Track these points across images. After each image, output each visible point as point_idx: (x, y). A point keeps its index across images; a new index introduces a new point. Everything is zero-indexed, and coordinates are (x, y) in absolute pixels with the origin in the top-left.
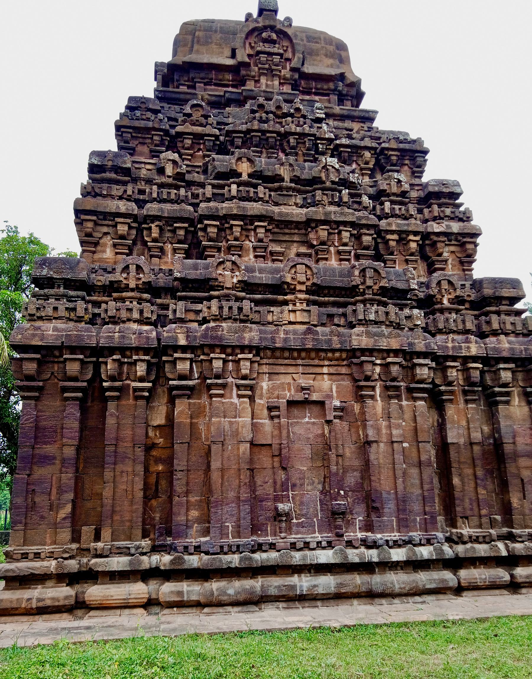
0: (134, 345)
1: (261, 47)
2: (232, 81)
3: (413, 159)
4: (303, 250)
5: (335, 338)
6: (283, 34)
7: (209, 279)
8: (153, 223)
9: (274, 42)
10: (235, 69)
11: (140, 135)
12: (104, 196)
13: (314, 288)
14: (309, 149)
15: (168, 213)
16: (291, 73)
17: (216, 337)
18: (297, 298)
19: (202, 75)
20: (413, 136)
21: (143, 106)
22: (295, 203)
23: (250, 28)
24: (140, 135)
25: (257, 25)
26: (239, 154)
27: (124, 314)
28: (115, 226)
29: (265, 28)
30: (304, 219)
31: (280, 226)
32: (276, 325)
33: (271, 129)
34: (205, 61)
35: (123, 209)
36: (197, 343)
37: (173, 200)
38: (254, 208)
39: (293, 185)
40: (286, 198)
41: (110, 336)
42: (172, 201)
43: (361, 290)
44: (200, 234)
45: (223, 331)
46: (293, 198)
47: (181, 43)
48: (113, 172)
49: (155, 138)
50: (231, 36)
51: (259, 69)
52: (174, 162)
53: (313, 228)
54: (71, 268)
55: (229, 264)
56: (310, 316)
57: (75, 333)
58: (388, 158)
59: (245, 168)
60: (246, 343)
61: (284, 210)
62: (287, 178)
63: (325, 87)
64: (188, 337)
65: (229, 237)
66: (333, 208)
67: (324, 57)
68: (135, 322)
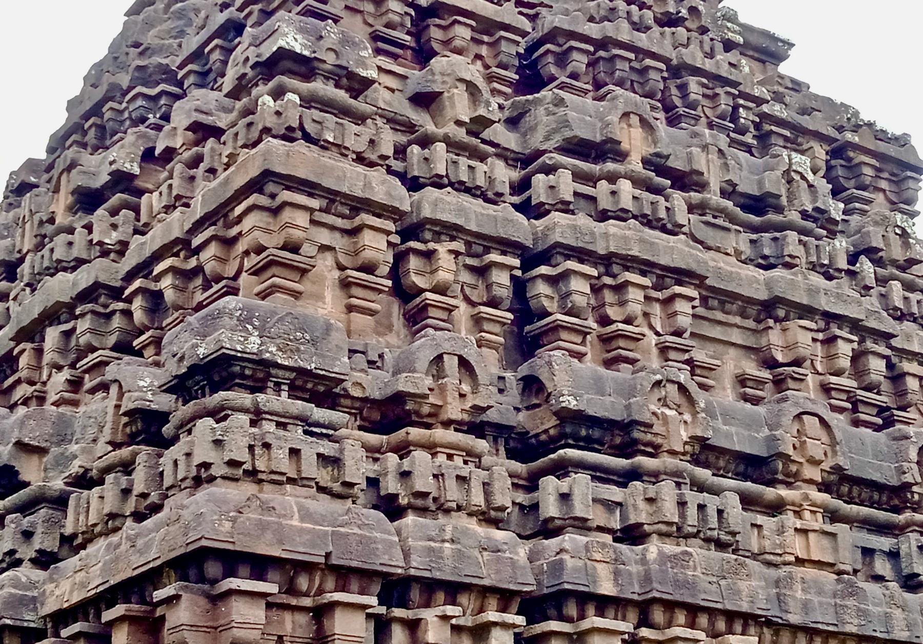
0: (486, 582)
3: (898, 182)
4: (751, 368)
5: (898, 613)
7: (634, 423)
8: (438, 241)
12: (325, 146)
13: (832, 477)
14: (722, 117)
17: (679, 584)
18: (806, 497)
20: (894, 129)
22: (736, 250)
26: (626, 103)
27: (453, 493)
28: (354, 232)
30: (763, 295)
32: (769, 564)
35: (379, 195)
36: (633, 592)
38: (673, 251)
39: (729, 204)
40: (721, 233)
41: (431, 550)
43: (916, 497)
44: (542, 288)
45: (695, 569)
46: (732, 236)
48: (331, 83)
52: (472, 88)
53: (777, 320)
54: (313, 342)
55: (672, 389)
56: (836, 550)
57: (356, 530)
58: (853, 169)
59: (635, 143)
60: (745, 607)
61: (722, 265)
62: (715, 185)
64: (616, 574)
66: (817, 279)
68: (470, 515)
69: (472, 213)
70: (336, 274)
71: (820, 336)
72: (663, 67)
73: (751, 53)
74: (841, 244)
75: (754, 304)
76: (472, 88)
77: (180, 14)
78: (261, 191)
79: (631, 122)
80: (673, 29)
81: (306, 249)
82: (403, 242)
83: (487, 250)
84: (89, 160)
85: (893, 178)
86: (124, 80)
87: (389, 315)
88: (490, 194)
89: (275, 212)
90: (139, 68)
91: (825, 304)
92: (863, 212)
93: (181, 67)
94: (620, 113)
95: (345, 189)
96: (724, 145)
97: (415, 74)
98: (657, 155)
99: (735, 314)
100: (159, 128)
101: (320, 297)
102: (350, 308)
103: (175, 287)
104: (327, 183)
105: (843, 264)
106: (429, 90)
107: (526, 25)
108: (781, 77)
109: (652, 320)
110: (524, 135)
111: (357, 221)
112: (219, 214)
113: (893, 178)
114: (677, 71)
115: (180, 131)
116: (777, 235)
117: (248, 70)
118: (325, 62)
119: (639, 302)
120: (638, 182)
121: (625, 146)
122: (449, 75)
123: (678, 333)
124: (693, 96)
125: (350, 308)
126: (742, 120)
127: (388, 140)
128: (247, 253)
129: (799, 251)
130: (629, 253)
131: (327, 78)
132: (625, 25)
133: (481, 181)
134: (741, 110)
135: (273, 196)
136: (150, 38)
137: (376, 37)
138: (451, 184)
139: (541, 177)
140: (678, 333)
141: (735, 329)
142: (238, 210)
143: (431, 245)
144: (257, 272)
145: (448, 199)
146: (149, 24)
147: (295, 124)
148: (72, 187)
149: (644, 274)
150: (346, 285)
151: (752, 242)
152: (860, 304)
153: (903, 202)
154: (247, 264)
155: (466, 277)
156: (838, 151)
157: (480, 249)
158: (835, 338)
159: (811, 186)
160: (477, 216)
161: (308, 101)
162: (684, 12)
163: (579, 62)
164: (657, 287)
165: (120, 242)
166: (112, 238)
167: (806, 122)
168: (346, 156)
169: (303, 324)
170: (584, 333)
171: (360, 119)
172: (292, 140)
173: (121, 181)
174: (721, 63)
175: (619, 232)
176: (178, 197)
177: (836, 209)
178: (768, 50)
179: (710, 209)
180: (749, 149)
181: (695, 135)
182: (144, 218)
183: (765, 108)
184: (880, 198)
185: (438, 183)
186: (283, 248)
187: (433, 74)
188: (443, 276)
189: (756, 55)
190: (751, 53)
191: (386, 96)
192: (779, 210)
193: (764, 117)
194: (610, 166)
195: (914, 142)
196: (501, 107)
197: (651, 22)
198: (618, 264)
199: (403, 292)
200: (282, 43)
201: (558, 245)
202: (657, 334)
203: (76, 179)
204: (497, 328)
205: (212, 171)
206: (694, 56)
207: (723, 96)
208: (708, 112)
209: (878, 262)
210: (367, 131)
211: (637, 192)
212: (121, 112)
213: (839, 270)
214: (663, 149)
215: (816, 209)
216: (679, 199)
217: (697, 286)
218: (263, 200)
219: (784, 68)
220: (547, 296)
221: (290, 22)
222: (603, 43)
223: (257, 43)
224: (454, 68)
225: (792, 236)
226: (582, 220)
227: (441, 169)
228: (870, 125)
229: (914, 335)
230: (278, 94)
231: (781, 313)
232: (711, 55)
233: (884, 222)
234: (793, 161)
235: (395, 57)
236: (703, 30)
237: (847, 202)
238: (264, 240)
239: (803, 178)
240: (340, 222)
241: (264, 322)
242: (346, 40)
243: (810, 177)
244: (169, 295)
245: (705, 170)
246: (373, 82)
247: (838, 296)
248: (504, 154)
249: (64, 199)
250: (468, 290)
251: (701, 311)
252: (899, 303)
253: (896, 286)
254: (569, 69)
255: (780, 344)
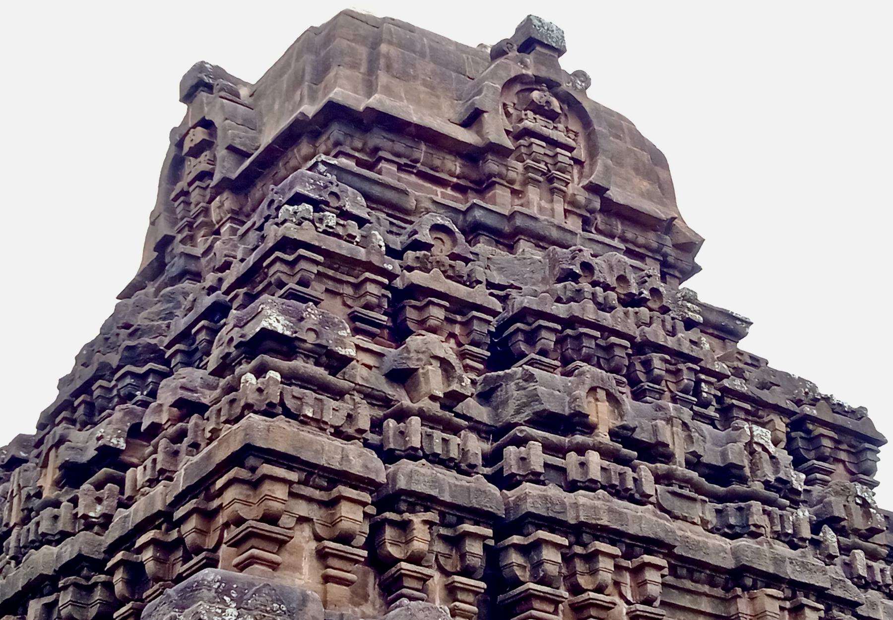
1: (532, 122)
2: (458, 177)
6: (574, 106)
8: (413, 511)
9: (552, 116)
10: (472, 156)
11: (331, 273)
12: (304, 421)
14: (685, 391)
15: (452, 497)
16: (586, 194)
19: (400, 147)
20: (851, 401)
21: (334, 203)
22: (702, 519)
23: (513, 75)
24: (331, 273)
25: (524, 72)
28: (332, 504)
29: (538, 81)
30: (730, 564)
31: (679, 571)
33: (619, 328)
34: (415, 119)
35: (356, 467)
37: (452, 459)
38: (642, 520)
39: (695, 475)
40: (686, 504)
42: (447, 463)
44: (515, 558)
46: (698, 505)
47: (347, 59)
48: (311, 361)
49: (371, 288)
50: (454, 75)
51: (527, 168)
52: (445, 364)
53: (745, 589)
58: (813, 441)
59: (602, 416)
61: (689, 534)
63: (641, 240)
65: (582, 581)
66: (782, 549)
67: (633, 173)
69: (446, 484)
70: (314, 545)
71: (788, 605)
72: (627, 343)
73: (711, 331)
74: (804, 514)
75: (723, 573)
76: (445, 364)
77: (170, 298)
78: (242, 466)
79: (598, 396)
80: (636, 309)
81: (285, 520)
82: (379, 513)
83: (461, 521)
84: (77, 436)
85: (852, 450)
86: (114, 359)
87: (365, 585)
88: (463, 466)
89: (255, 485)
90: (128, 348)
91: (791, 572)
92: (825, 483)
93: (169, 346)
94: (587, 387)
95: (323, 462)
96: (688, 420)
97: (391, 352)
98: (624, 427)
99: (703, 584)
100: (145, 404)
101: (297, 568)
102: (327, 579)
103: (155, 559)
104: (304, 456)
105: (806, 533)
106: (405, 366)
107: (497, 306)
108: (741, 353)
109: (623, 588)
110: (496, 409)
111: (335, 492)
112: (202, 487)
113: (852, 450)
114: (642, 347)
115: (165, 408)
116: (742, 504)
117: (232, 349)
118: (305, 341)
119: (607, 570)
120: (605, 454)
121: (593, 418)
122: (423, 352)
123: (649, 601)
124: (656, 372)
125: (327, 579)
126: (705, 395)
127: (365, 415)
128: (226, 525)
129: (764, 521)
130: (599, 522)
131: (308, 357)
132: (591, 305)
133: (454, 453)
134: (703, 385)
135: (253, 470)
136: (140, 320)
137: (353, 318)
138: (426, 457)
139: (512, 448)
140: (649, 601)
141: (705, 599)
142: (219, 483)
143: (406, 516)
144: (236, 544)
145: (423, 470)
146: (140, 307)
147: (276, 400)
148: (59, 462)
149: (613, 543)
150: (322, 556)
151: (718, 511)
152: (824, 572)
153: (863, 472)
154: (226, 536)
155: (439, 547)
156: (798, 423)
157: (453, 519)
158: (802, 607)
159: (772, 457)
160: (450, 487)
161: (289, 378)
162: (646, 293)
163: (548, 340)
164: (627, 556)
165: (104, 515)
166: (96, 512)
167: (765, 395)
168: (325, 430)
169: (280, 596)
170: (555, 602)
171: (338, 394)
172: (273, 415)
173: (107, 455)
174: (683, 340)
175: (589, 502)
176: (162, 471)
177: (798, 480)
178: (727, 328)
179: (676, 479)
180: (711, 421)
181: (659, 408)
182: (128, 492)
183: (726, 383)
184: (839, 469)
185: (413, 455)
186: (262, 520)
187: (409, 352)
188: (419, 545)
189: (716, 333)
190: (711, 331)
191: (363, 372)
192: (743, 480)
193: (725, 391)
194: (579, 438)
195: (870, 415)
196: (474, 382)
197: (615, 302)
198: (587, 533)
199: (379, 562)
200: (264, 324)
201: (529, 514)
202: (628, 603)
203: (64, 454)
204: (471, 598)
205: (195, 446)
206: (657, 334)
207: (685, 371)
208: (672, 386)
209: (841, 531)
210: (345, 407)
211: (606, 463)
212: (110, 390)
213: (804, 540)
214: (629, 421)
215: (778, 480)
216: (645, 470)
217: (665, 556)
218: (244, 474)
219: (743, 345)
220: (519, 565)
221: (272, 305)
222: (572, 322)
223: (241, 324)
224: (428, 346)
225: (757, 506)
226: (553, 491)
227: (416, 441)
228: (827, 399)
229: (879, 603)
230: (259, 372)
231: (749, 582)
232: (673, 333)
233: (844, 492)
234: (755, 433)
235: (372, 336)
236: (665, 310)
237: (807, 472)
238: (244, 512)
239: (765, 449)
240: (317, 494)
241: (242, 593)
242: (326, 321)
243: (772, 448)
244: (150, 567)
245: (669, 441)
246: (351, 359)
247: (804, 565)
248: (477, 427)
249: (51, 474)
250: (442, 560)
251: (670, 580)
252: (863, 572)
253: (859, 555)
254: (538, 347)
255: (749, 613)
